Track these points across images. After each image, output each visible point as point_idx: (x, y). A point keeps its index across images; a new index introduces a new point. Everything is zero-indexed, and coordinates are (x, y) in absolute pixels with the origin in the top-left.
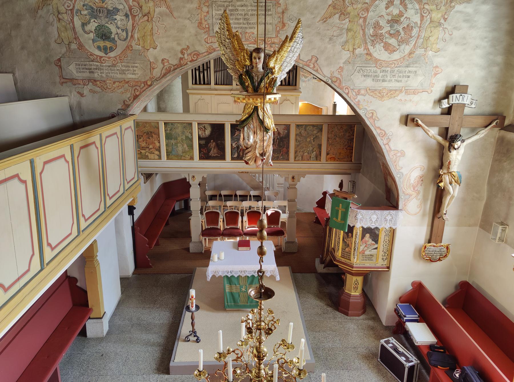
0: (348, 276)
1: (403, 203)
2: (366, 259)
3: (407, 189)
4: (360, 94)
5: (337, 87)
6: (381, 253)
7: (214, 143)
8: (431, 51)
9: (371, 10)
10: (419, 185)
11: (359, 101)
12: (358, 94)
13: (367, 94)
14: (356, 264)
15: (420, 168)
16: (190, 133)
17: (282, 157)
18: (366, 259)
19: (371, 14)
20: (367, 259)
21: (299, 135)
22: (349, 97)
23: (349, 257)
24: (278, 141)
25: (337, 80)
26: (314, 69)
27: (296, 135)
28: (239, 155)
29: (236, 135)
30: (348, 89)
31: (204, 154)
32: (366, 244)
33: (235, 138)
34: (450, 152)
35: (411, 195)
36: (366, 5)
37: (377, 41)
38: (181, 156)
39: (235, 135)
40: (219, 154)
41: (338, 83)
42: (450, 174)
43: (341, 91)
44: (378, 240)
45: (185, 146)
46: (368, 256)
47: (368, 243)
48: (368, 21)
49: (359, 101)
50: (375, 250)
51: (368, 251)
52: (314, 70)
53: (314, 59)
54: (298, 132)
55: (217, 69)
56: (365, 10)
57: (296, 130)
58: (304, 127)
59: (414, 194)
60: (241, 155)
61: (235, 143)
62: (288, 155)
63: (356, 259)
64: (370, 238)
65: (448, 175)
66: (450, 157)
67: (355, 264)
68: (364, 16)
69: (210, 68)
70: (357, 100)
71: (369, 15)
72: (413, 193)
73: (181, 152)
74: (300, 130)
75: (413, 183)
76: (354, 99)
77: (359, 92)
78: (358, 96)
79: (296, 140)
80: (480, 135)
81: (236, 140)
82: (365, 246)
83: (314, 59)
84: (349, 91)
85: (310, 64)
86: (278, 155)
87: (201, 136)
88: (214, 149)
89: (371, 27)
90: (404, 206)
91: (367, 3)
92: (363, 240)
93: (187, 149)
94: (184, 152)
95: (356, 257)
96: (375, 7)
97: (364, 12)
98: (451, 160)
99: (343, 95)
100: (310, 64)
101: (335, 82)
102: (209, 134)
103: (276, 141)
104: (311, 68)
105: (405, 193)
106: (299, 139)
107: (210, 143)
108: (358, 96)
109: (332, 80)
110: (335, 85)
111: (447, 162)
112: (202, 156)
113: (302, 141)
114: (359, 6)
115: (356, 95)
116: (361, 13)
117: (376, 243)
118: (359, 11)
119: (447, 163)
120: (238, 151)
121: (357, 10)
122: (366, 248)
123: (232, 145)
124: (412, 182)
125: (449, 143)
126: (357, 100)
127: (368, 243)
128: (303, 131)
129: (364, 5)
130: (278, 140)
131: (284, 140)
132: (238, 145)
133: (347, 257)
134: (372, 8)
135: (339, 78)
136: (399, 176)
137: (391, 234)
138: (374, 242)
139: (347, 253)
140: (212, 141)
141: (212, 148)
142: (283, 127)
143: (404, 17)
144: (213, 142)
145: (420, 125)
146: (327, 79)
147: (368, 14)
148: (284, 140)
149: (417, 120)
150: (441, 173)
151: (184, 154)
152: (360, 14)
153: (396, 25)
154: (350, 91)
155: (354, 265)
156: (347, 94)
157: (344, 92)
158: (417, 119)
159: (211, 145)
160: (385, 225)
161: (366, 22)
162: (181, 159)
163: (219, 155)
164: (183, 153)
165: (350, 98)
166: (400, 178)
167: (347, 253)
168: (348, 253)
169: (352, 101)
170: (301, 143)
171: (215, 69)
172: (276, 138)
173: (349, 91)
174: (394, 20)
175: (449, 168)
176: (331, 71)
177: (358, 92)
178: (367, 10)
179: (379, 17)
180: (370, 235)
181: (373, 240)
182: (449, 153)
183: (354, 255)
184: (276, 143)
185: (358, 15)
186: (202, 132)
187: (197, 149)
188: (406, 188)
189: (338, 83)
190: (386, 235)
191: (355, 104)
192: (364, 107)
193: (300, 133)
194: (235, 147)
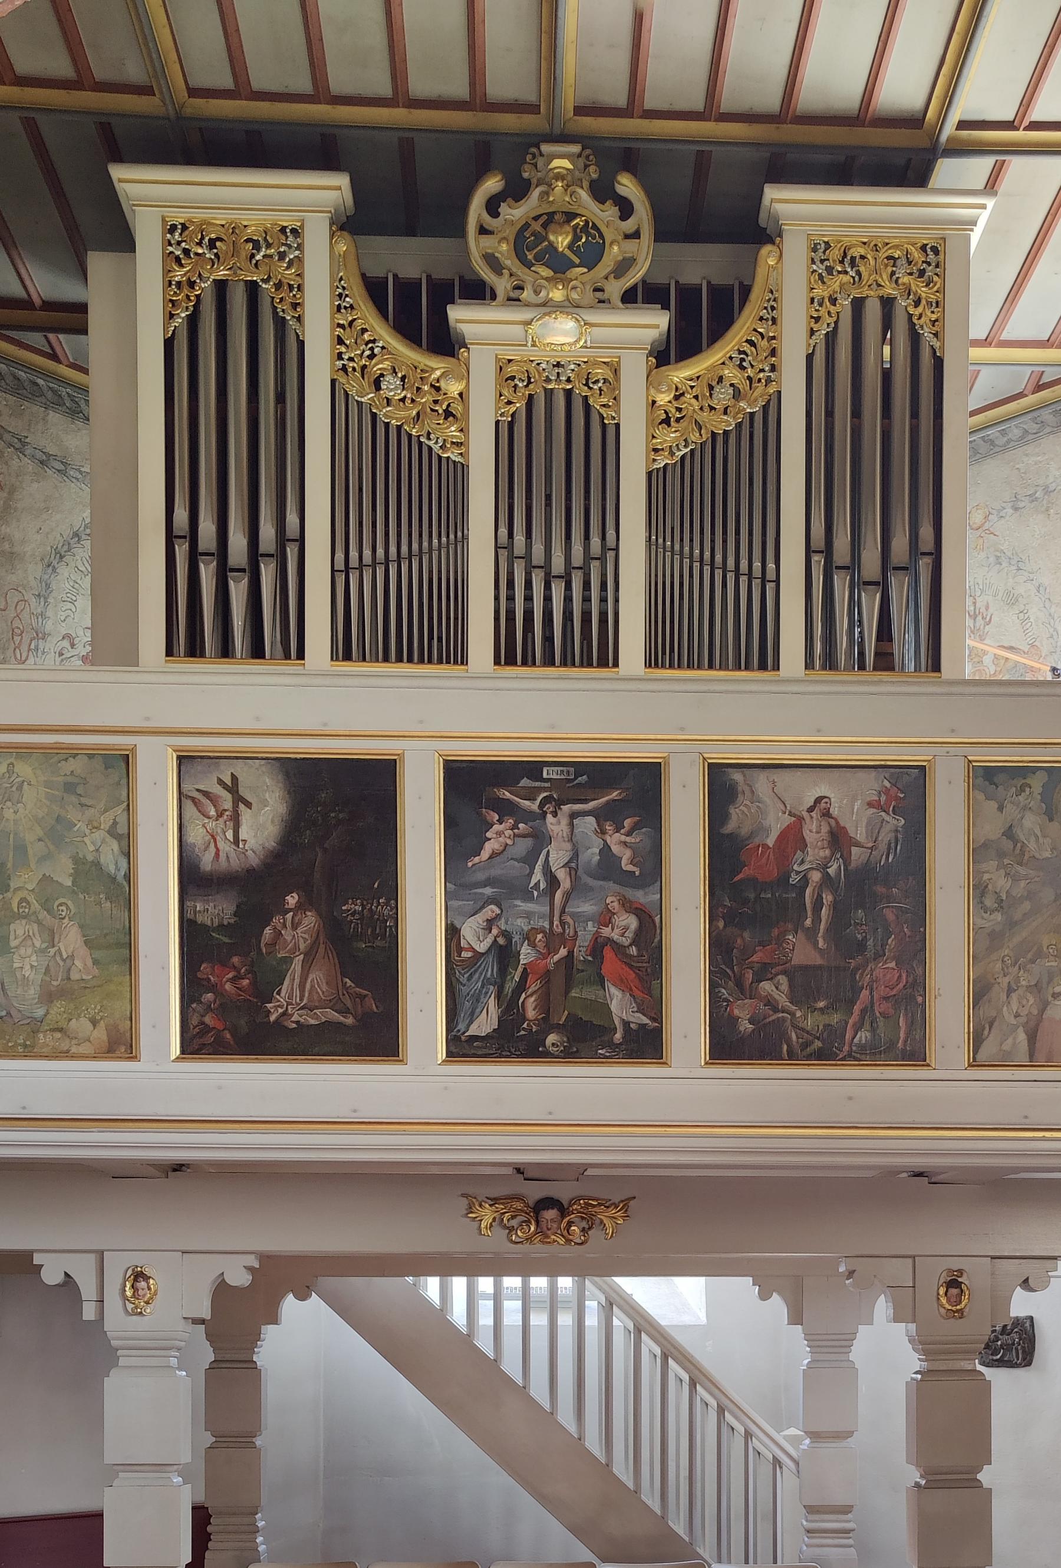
7: (310, 920)
16: (118, 837)
17: (863, 1036)
21: (1001, 855)
24: (828, 898)
27: (978, 852)
28: (510, 1012)
29: (488, 848)
31: (224, 1008)
33: (481, 876)
38: (35, 1026)
39: (485, 854)
40: (344, 1011)
45: (71, 940)
54: (992, 828)
55: (354, 554)
57: (973, 813)
58: (1037, 783)
60: (531, 1013)
61: (480, 919)
62: (919, 1021)
69: (301, 540)
73: (33, 992)
74: (1009, 808)
79: (980, 890)
81: (488, 891)
86: (835, 1018)
87: (207, 862)
88: (310, 956)
93: (82, 967)
94: (62, 993)
102: (271, 844)
103: (818, 905)
106: (1001, 883)
107: (277, 920)
112: (205, 1029)
113: (1030, 896)
120: (509, 987)
123: (452, 933)
128: (1031, 822)
130: (835, 891)
131: (880, 889)
132: (505, 934)
140: (292, 900)
141: (288, 961)
142: (871, 786)
144: (300, 907)
148: (880, 889)
151: (58, 1007)
159: (287, 934)
162: (29, 1052)
163: (350, 1021)
164: (48, 997)
170: (1018, 915)
171: (340, 556)
172: (816, 876)
184: (817, 919)
186: (211, 825)
187: (165, 968)
193: (1009, 833)
194: (482, 948)
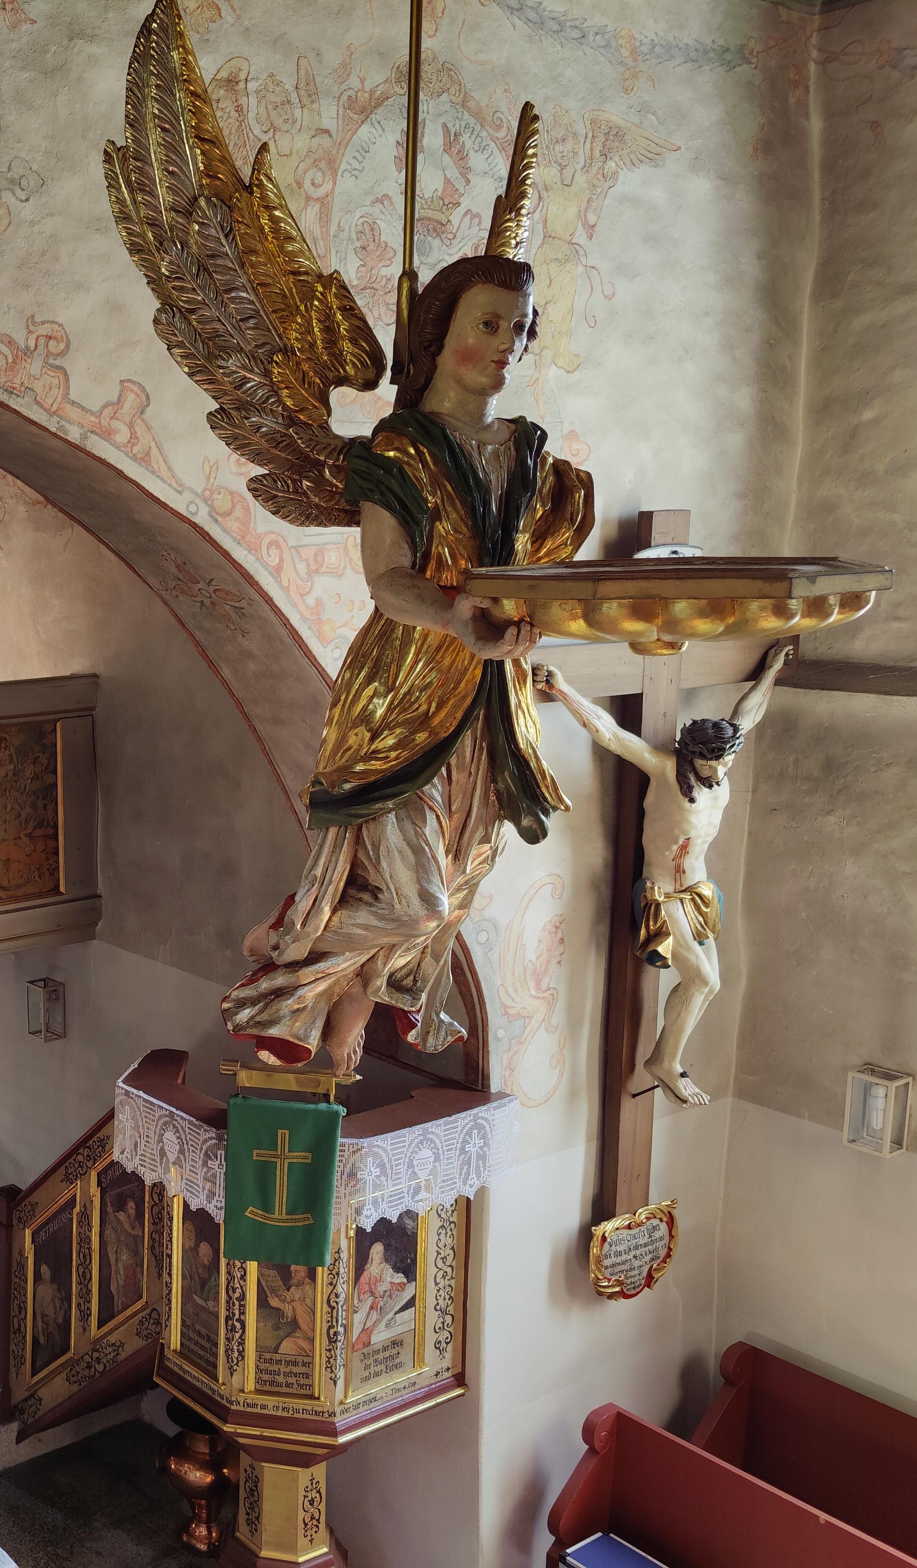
0: (271, 1472)
1: (505, 1062)
2: (378, 1368)
3: (516, 991)
4: (324, 569)
5: (235, 539)
6: (433, 1318)
8: (553, 368)
9: (343, 166)
10: (554, 961)
11: (319, 603)
12: (317, 571)
13: (349, 570)
14: (342, 1412)
15: (550, 887)
18: (378, 1368)
19: (345, 184)
20: (383, 1367)
22: (281, 586)
23: (303, 1381)
25: (234, 506)
26: (136, 449)
30: (278, 547)
32: (372, 1294)
34: (692, 800)
35: (530, 1017)
36: (325, 141)
37: (376, 315)
41: (237, 519)
42: (687, 896)
43: (251, 558)
44: (414, 1261)
46: (385, 1349)
47: (382, 1287)
48: (335, 216)
49: (319, 603)
50: (410, 1312)
51: (383, 1323)
52: (134, 458)
53: (131, 400)
56: (323, 165)
59: (538, 1007)
63: (341, 1383)
64: (387, 1261)
65: (681, 900)
66: (690, 823)
67: (338, 1410)
68: (321, 192)
70: (311, 601)
71: (337, 191)
72: (537, 1003)
75: (534, 960)
76: (302, 595)
77: (319, 559)
78: (316, 579)
80: (753, 713)
82: (371, 1308)
83: (131, 400)
84: (281, 560)
85: (116, 424)
89: (351, 247)
90: (507, 1073)
91: (327, 131)
92: (362, 1280)
95: (341, 1374)
96: (358, 155)
97: (319, 174)
98: (692, 834)
99: (257, 577)
100: (116, 424)
101: (229, 514)
104: (118, 448)
105: (511, 1012)
108: (316, 579)
109: (211, 506)
110: (225, 531)
111: (676, 843)
114: (301, 142)
115: (313, 573)
116: (309, 176)
117: (407, 1277)
118: (302, 167)
119: (675, 848)
121: (294, 161)
122: (374, 1316)
124: (531, 955)
125: (675, 760)
126: (311, 601)
127: (382, 1287)
129: (317, 140)
133: (288, 1385)
134: (348, 157)
135: (240, 495)
136: (483, 937)
137: (458, 1216)
138: (400, 1278)
139: (288, 1363)
143: (461, 210)
145: (561, 691)
146: (191, 502)
147: (335, 184)
149: (550, 674)
150: (657, 898)
152: (307, 184)
153: (436, 242)
154: (287, 555)
155: (340, 1421)
156: (277, 571)
157: (265, 566)
158: (551, 668)
160: (465, 1183)
161: (328, 222)
165: (286, 590)
166: (488, 947)
167: (288, 1363)
168: (295, 1363)
169: (295, 606)
173: (281, 560)
174: (429, 219)
175: (679, 871)
176: (206, 459)
177: (316, 561)
178: (330, 164)
179: (377, 200)
180: (387, 1248)
181: (397, 1269)
182: (687, 804)
183: (331, 1368)
185: (299, 185)
188: (511, 991)
189: (237, 519)
190: (442, 1227)
191: (302, 616)
192: (339, 632)
